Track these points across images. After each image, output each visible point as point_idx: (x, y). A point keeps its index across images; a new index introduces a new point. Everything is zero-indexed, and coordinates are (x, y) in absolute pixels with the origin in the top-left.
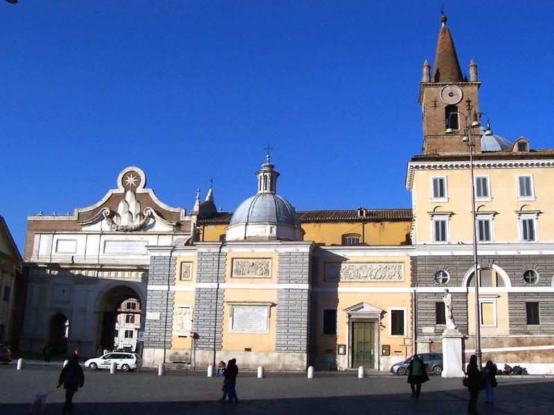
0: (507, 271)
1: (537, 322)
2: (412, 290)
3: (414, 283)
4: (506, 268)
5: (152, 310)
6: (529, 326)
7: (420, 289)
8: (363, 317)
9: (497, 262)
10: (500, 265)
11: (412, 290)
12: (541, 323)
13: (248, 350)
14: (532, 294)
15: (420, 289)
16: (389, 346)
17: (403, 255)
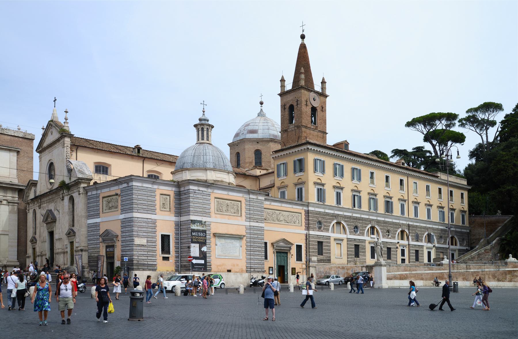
0: (348, 225)
1: (358, 257)
2: (305, 232)
3: (308, 228)
4: (347, 223)
5: (138, 236)
6: (356, 258)
7: (311, 232)
8: (282, 248)
9: (344, 219)
10: (345, 221)
11: (305, 232)
12: (360, 257)
13: (229, 271)
14: (357, 240)
15: (311, 232)
16: (295, 268)
17: (301, 209)
